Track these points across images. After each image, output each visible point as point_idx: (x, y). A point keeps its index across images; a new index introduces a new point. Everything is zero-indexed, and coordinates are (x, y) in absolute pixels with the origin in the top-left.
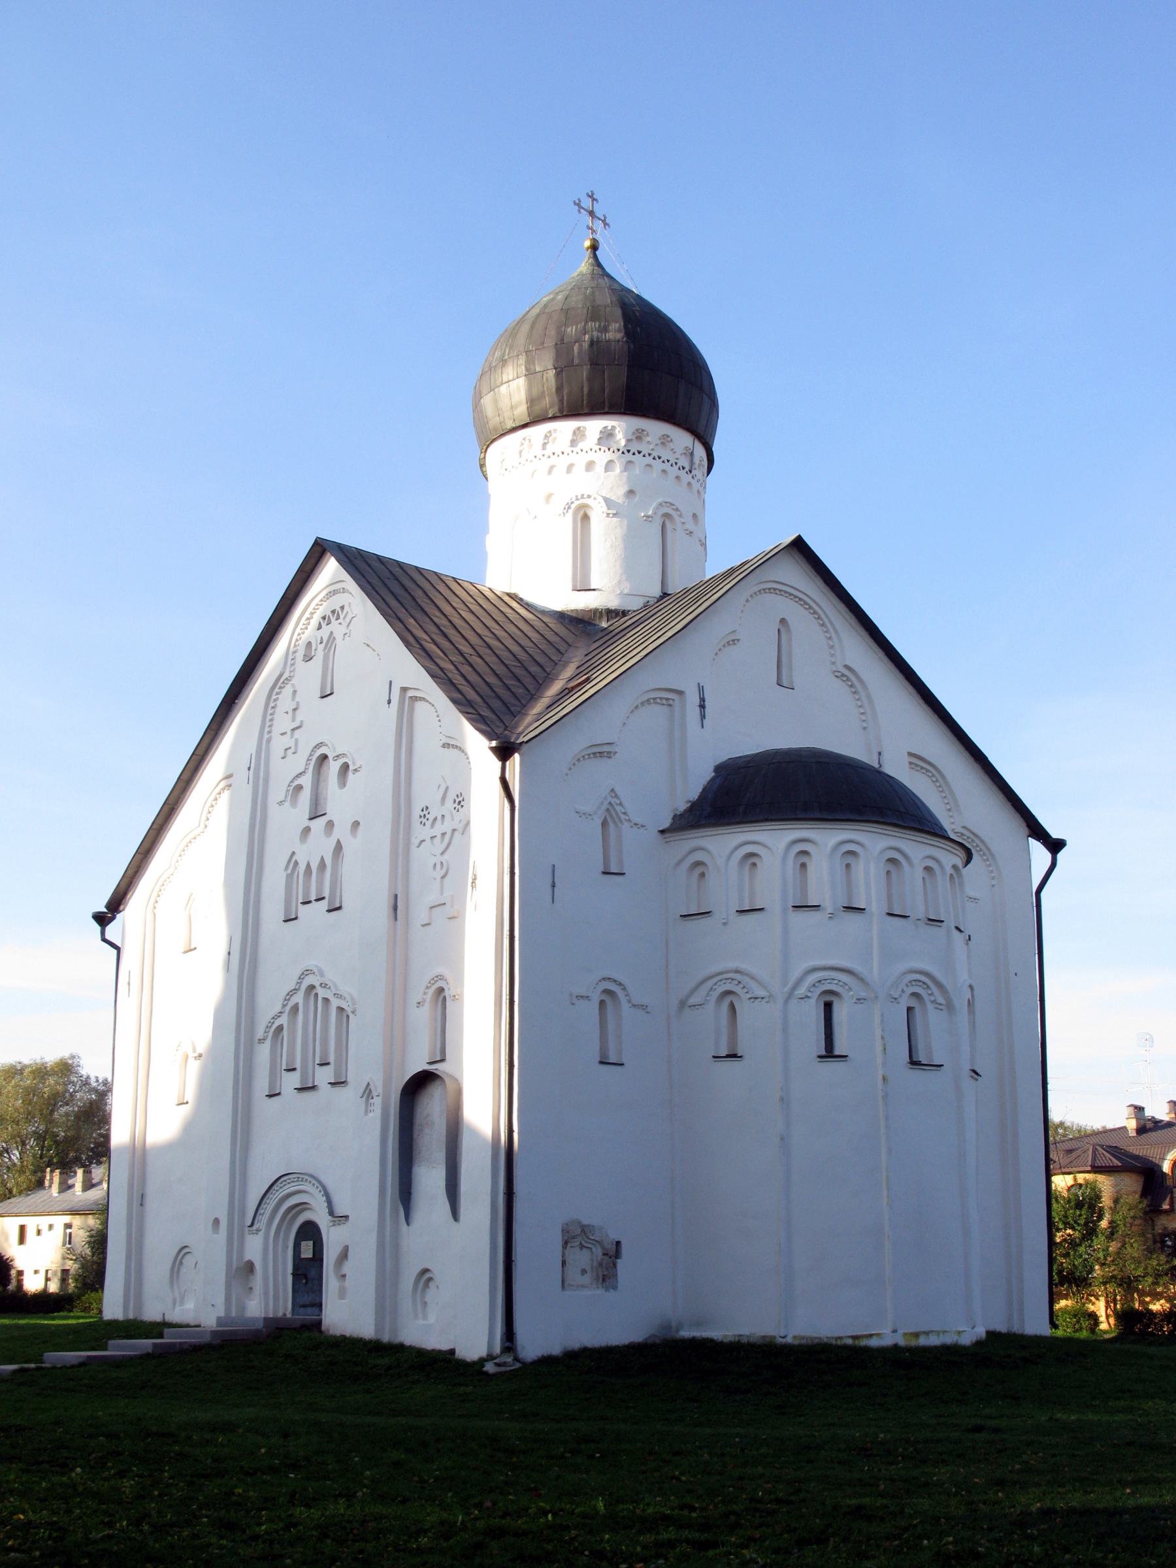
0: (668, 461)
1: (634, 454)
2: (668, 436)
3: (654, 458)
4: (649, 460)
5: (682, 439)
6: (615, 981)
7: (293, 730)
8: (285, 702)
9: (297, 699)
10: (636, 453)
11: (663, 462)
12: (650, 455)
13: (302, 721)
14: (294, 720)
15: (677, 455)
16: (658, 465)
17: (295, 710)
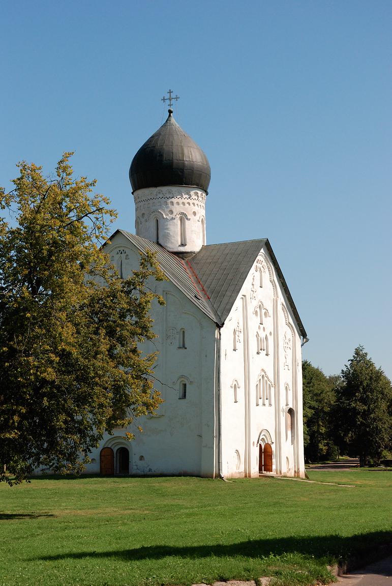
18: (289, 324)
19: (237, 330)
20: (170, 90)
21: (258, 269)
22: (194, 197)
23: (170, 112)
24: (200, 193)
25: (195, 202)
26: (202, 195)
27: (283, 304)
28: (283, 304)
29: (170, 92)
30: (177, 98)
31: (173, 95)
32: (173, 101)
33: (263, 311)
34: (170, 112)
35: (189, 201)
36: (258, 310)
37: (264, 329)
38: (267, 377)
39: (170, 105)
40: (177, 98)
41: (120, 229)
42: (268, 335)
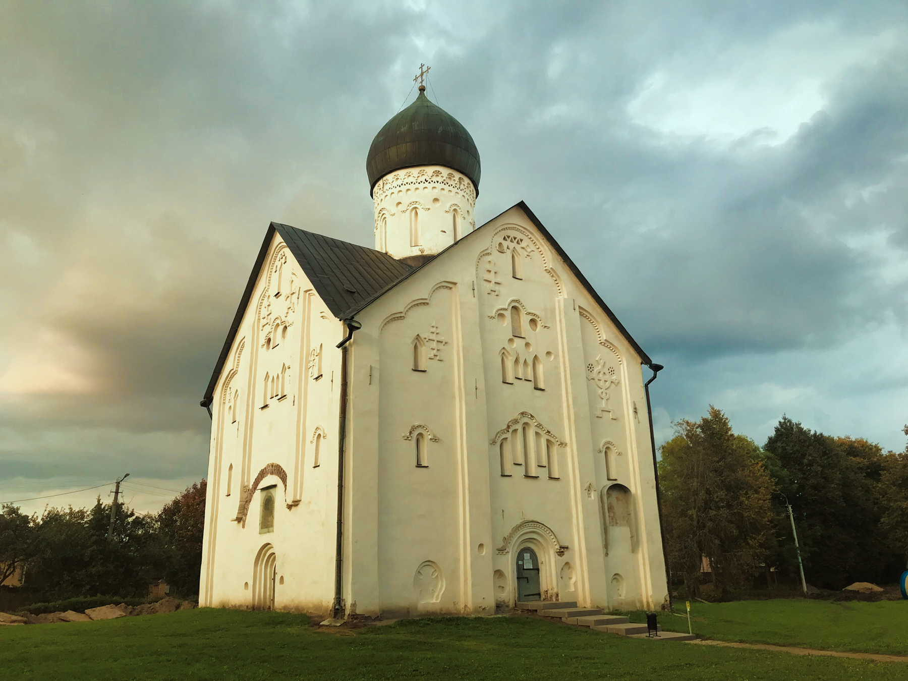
0: (452, 185)
1: (435, 182)
2: (452, 174)
3: (445, 184)
4: (442, 186)
5: (457, 175)
6: (420, 426)
7: (268, 315)
8: (265, 303)
9: (270, 300)
10: (436, 182)
11: (449, 186)
12: (443, 183)
13: (271, 310)
14: (268, 311)
15: (456, 182)
16: (446, 187)
17: (269, 305)
18: (606, 344)
19: (433, 337)
20: (421, 65)
21: (509, 253)
22: (435, 179)
23: (422, 89)
24: (445, 171)
25: (436, 185)
26: (450, 176)
27: (580, 307)
28: (580, 307)
29: (422, 66)
30: (428, 69)
31: (425, 69)
32: (424, 77)
33: (525, 320)
34: (422, 89)
35: (427, 184)
36: (508, 314)
37: (527, 345)
38: (539, 426)
39: (422, 81)
40: (428, 69)
41: (278, 220)
42: (542, 356)
